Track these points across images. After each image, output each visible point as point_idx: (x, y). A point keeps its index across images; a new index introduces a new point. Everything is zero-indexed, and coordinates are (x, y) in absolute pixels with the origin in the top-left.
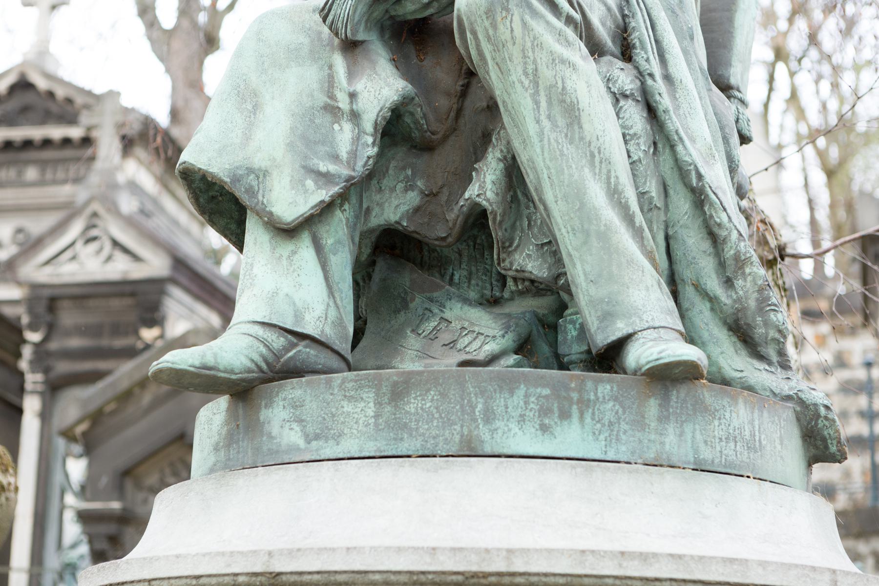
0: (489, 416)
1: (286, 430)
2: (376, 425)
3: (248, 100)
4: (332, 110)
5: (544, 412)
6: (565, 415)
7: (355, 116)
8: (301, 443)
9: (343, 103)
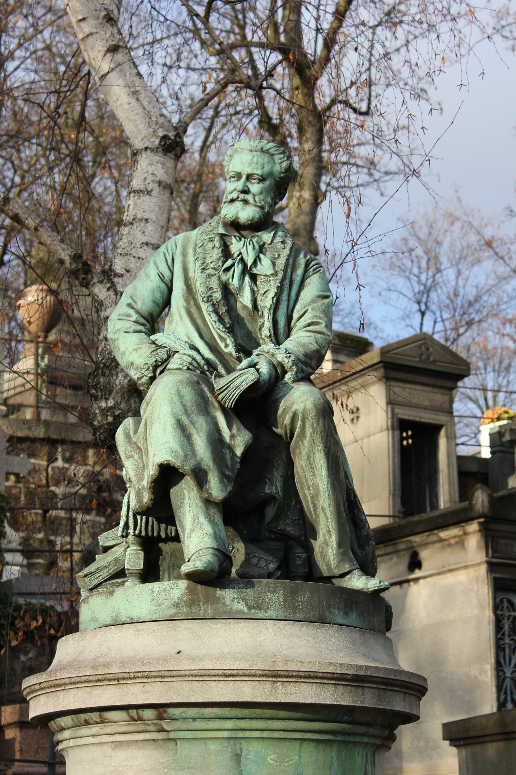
0: (329, 607)
1: (235, 603)
2: (284, 605)
3: (183, 431)
5: (346, 606)
6: (352, 609)
8: (245, 610)
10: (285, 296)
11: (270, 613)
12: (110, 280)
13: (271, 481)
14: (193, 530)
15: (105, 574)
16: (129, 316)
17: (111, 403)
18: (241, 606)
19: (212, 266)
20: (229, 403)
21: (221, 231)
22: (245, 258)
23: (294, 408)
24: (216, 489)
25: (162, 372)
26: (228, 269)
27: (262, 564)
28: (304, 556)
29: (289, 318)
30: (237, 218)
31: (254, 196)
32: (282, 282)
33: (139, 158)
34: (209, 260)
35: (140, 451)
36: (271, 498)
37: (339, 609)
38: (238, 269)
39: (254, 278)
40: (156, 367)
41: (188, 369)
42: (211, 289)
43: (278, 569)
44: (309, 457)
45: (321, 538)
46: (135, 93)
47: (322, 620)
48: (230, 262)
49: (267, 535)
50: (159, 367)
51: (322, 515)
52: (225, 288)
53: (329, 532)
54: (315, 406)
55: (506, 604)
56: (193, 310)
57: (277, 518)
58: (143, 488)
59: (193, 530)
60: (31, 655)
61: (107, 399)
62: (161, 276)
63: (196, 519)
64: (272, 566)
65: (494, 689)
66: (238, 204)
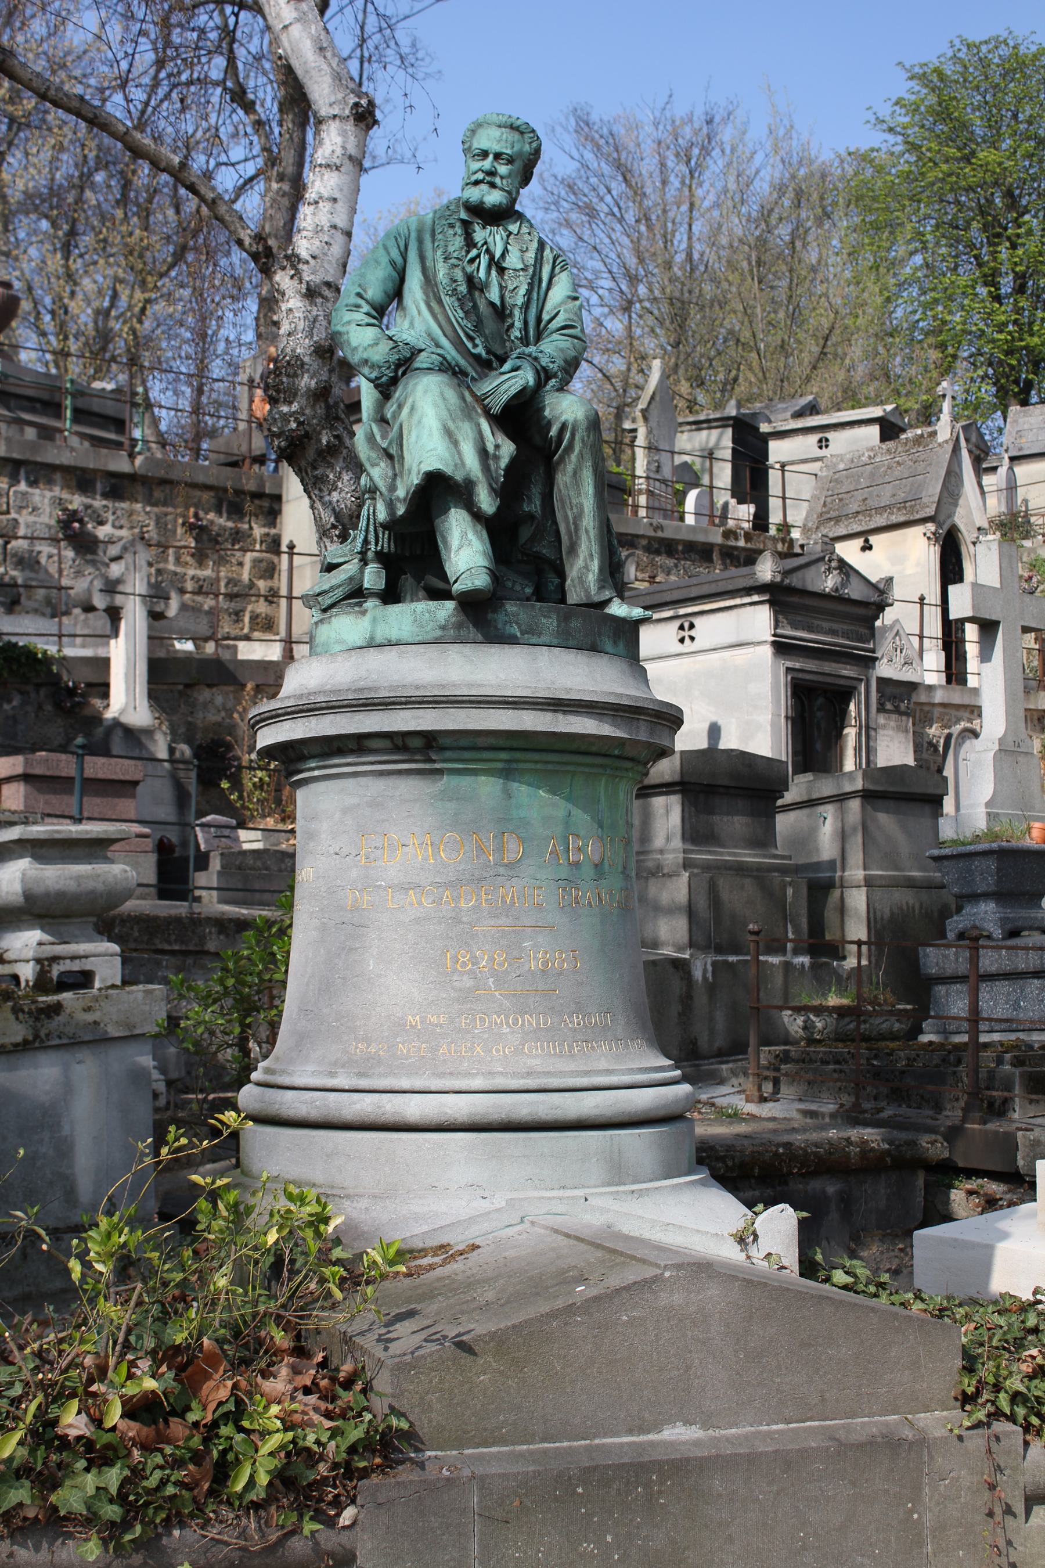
0: (600, 635)
1: (508, 627)
11: (544, 639)
12: (294, 267)
14: (460, 547)
15: (339, 593)
16: (358, 306)
17: (295, 407)
19: (455, 255)
20: (496, 410)
21: (463, 215)
22: (492, 248)
23: (563, 418)
24: (486, 501)
25: (404, 374)
26: (472, 261)
29: (539, 319)
30: (482, 203)
31: (502, 178)
33: (324, 127)
34: (451, 249)
35: (392, 457)
36: (531, 517)
38: (484, 260)
39: (501, 270)
40: (398, 366)
42: (455, 281)
44: (575, 473)
45: (580, 562)
46: (322, 49)
47: (594, 648)
48: (474, 252)
49: (520, 557)
51: (584, 537)
52: (470, 279)
53: (591, 555)
54: (587, 417)
56: (434, 304)
57: (532, 539)
58: (398, 499)
59: (460, 547)
60: (15, 703)
61: (290, 403)
62: (393, 263)
63: (464, 535)
64: (528, 590)
66: (484, 187)
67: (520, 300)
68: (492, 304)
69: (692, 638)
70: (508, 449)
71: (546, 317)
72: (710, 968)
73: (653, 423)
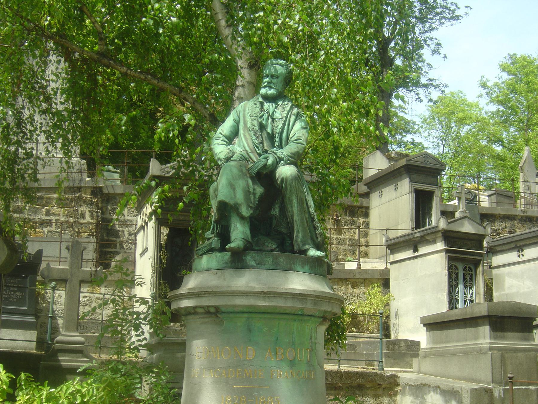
0: (294, 264)
1: (251, 262)
3: (232, 186)
4: (249, 191)
5: (302, 264)
7: (254, 194)
8: (255, 265)
9: (251, 190)
10: (286, 127)
13: (274, 209)
18: (253, 263)
23: (282, 177)
26: (261, 117)
27: (270, 245)
28: (290, 242)
31: (274, 84)
32: (285, 122)
37: (299, 265)
41: (239, 160)
43: (277, 247)
50: (228, 159)
55: (453, 267)
64: (274, 246)
65: (447, 303)
66: (267, 88)
67: (278, 130)
68: (268, 133)
69: (523, 255)
70: (259, 190)
71: (291, 136)
72: (502, 391)
73: (525, 171)
